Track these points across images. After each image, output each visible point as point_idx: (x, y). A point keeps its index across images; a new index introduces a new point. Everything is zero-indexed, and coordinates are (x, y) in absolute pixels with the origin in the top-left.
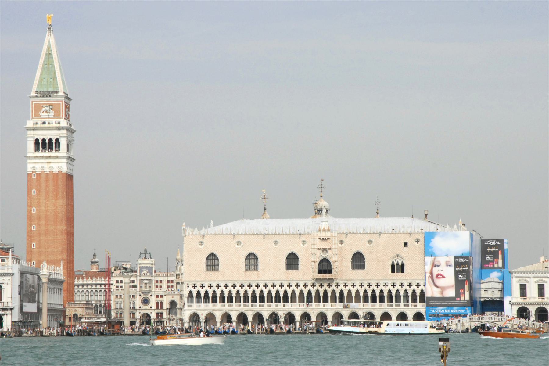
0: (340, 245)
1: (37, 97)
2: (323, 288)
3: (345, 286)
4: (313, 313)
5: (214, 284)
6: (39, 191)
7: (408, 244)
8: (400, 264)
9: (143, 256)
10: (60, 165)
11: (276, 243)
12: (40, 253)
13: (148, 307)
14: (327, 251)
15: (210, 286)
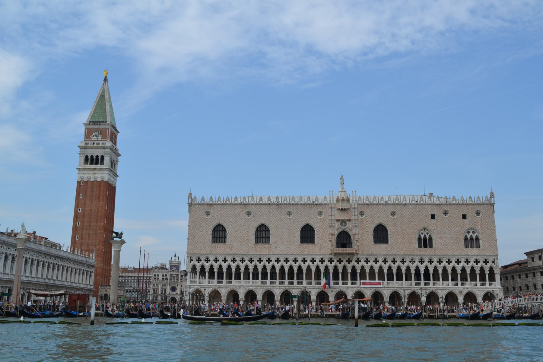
0: (360, 217)
1: (89, 124)
2: (343, 264)
3: (367, 261)
4: (332, 291)
5: (220, 258)
6: (85, 196)
7: (436, 217)
8: (428, 238)
9: (173, 258)
10: (103, 175)
11: (289, 214)
12: (81, 244)
13: (175, 293)
14: (346, 223)
15: (216, 260)
